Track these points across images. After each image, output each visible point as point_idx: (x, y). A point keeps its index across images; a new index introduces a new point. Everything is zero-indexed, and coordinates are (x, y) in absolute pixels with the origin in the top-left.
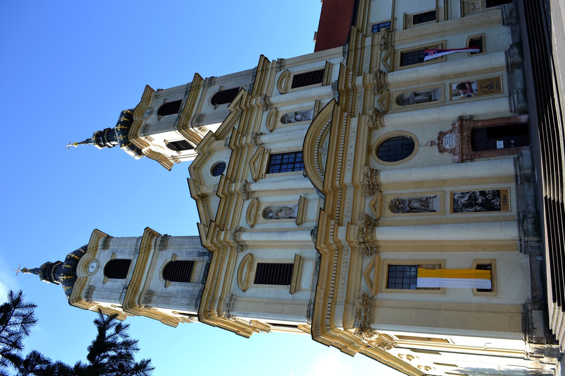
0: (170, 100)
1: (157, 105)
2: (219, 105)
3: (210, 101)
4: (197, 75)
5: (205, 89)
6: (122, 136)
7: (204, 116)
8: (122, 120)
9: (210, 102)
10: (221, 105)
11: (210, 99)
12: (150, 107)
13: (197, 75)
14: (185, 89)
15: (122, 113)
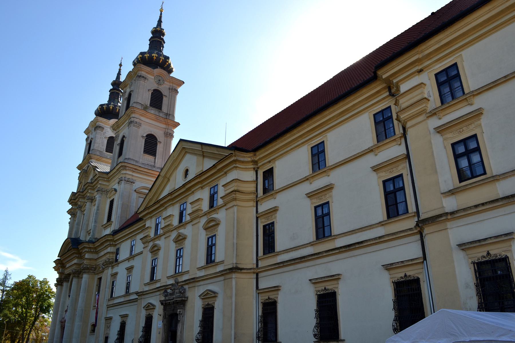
0: (165, 100)
1: (164, 89)
2: (144, 139)
3: (150, 133)
4: (178, 124)
5: (164, 129)
6: (148, 56)
7: (138, 128)
8: (161, 57)
9: (150, 133)
10: (144, 141)
11: (152, 133)
12: (164, 83)
13: (178, 124)
14: (169, 113)
15: (168, 58)
